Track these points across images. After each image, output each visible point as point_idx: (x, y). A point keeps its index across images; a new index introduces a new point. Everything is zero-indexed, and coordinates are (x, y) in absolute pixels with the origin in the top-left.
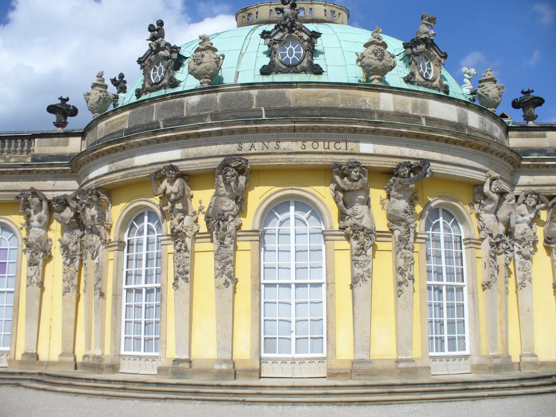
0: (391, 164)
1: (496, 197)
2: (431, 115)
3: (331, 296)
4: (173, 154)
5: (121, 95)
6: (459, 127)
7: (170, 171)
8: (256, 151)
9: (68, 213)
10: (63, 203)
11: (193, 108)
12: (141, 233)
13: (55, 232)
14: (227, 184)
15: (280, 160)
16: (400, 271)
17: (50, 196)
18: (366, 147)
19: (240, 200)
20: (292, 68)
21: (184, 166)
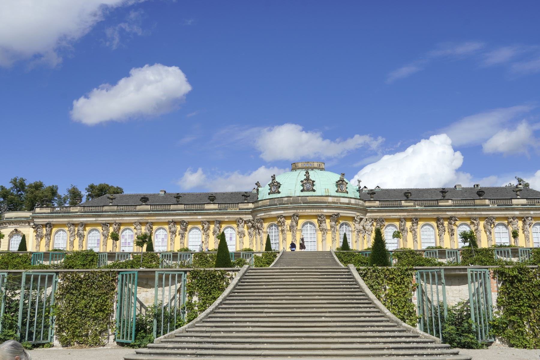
0: (331, 214)
1: (359, 220)
2: (341, 201)
3: (317, 244)
4: (282, 212)
5: (259, 189)
7: (280, 216)
8: (300, 212)
9: (250, 224)
10: (249, 221)
11: (285, 201)
12: (272, 229)
13: (245, 229)
14: (294, 219)
15: (306, 214)
16: (333, 238)
17: (245, 219)
18: (325, 211)
19: (297, 224)
20: (308, 190)
21: (284, 215)
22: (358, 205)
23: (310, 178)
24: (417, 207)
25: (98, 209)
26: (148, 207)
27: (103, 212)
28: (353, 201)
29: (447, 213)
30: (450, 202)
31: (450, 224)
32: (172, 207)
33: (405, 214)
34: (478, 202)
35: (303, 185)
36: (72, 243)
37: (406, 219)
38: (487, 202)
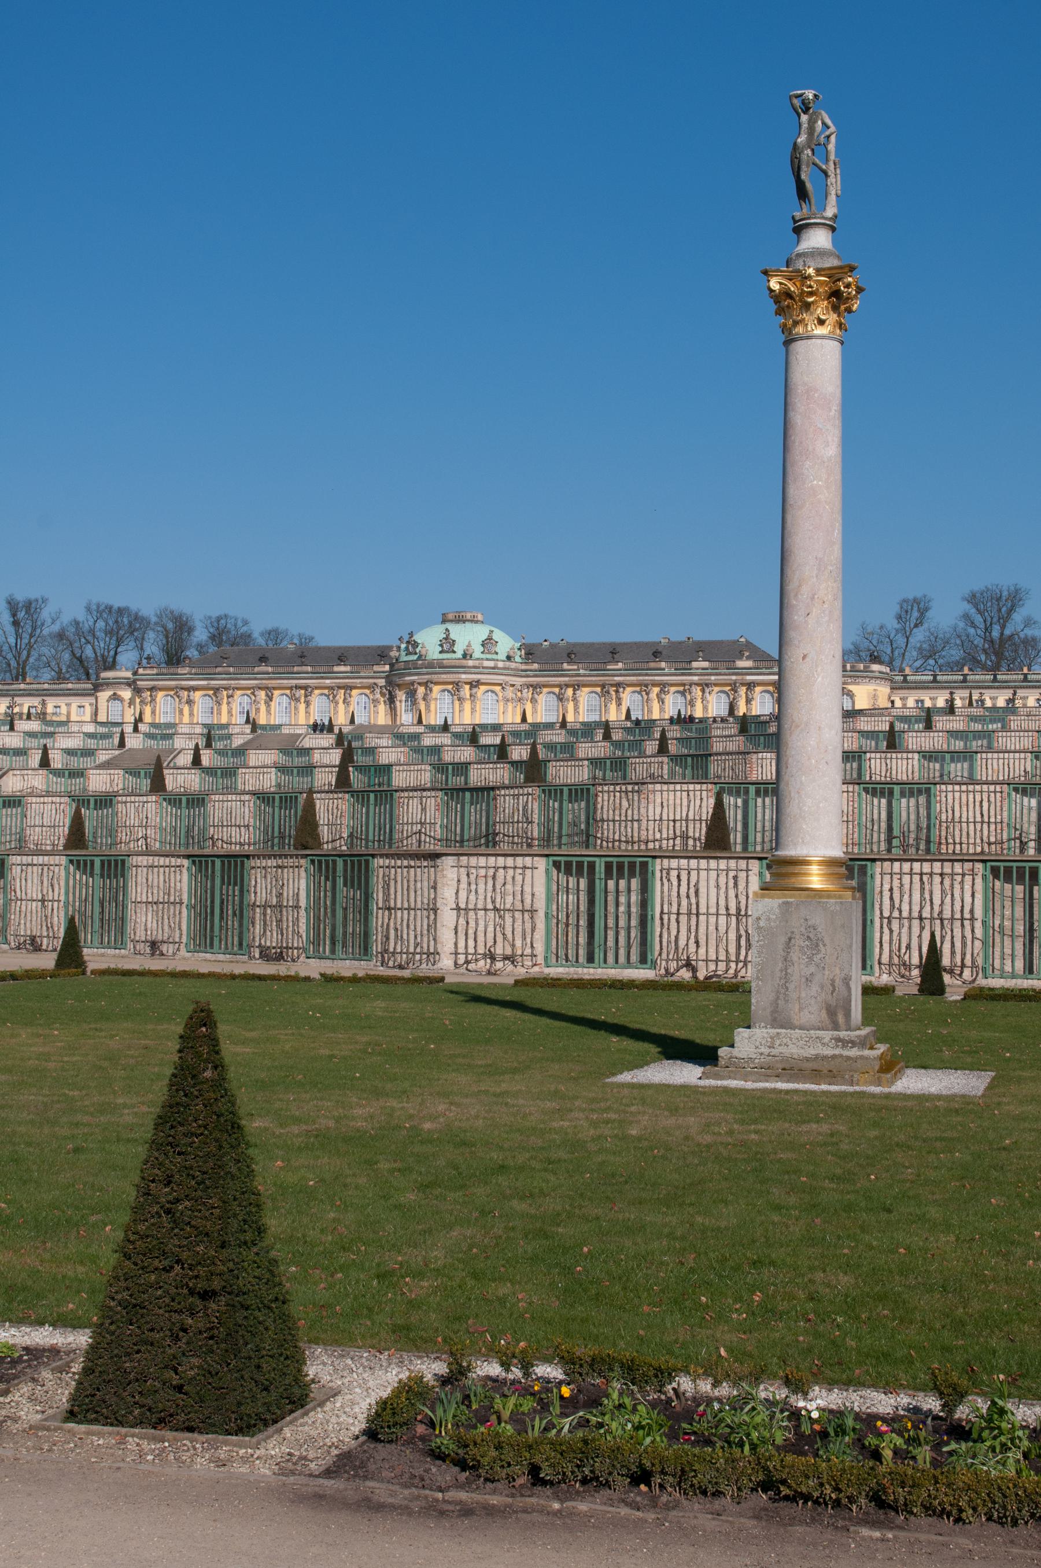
6: (493, 668)
20: (447, 652)
22: (508, 669)
23: (452, 636)
24: (582, 672)
25: (208, 671)
26: (270, 669)
27: (215, 674)
28: (500, 665)
29: (616, 678)
30: (620, 665)
31: (617, 692)
32: (296, 669)
33: (567, 679)
34: (652, 665)
35: (441, 645)
36: (181, 712)
37: (567, 686)
38: (663, 665)
